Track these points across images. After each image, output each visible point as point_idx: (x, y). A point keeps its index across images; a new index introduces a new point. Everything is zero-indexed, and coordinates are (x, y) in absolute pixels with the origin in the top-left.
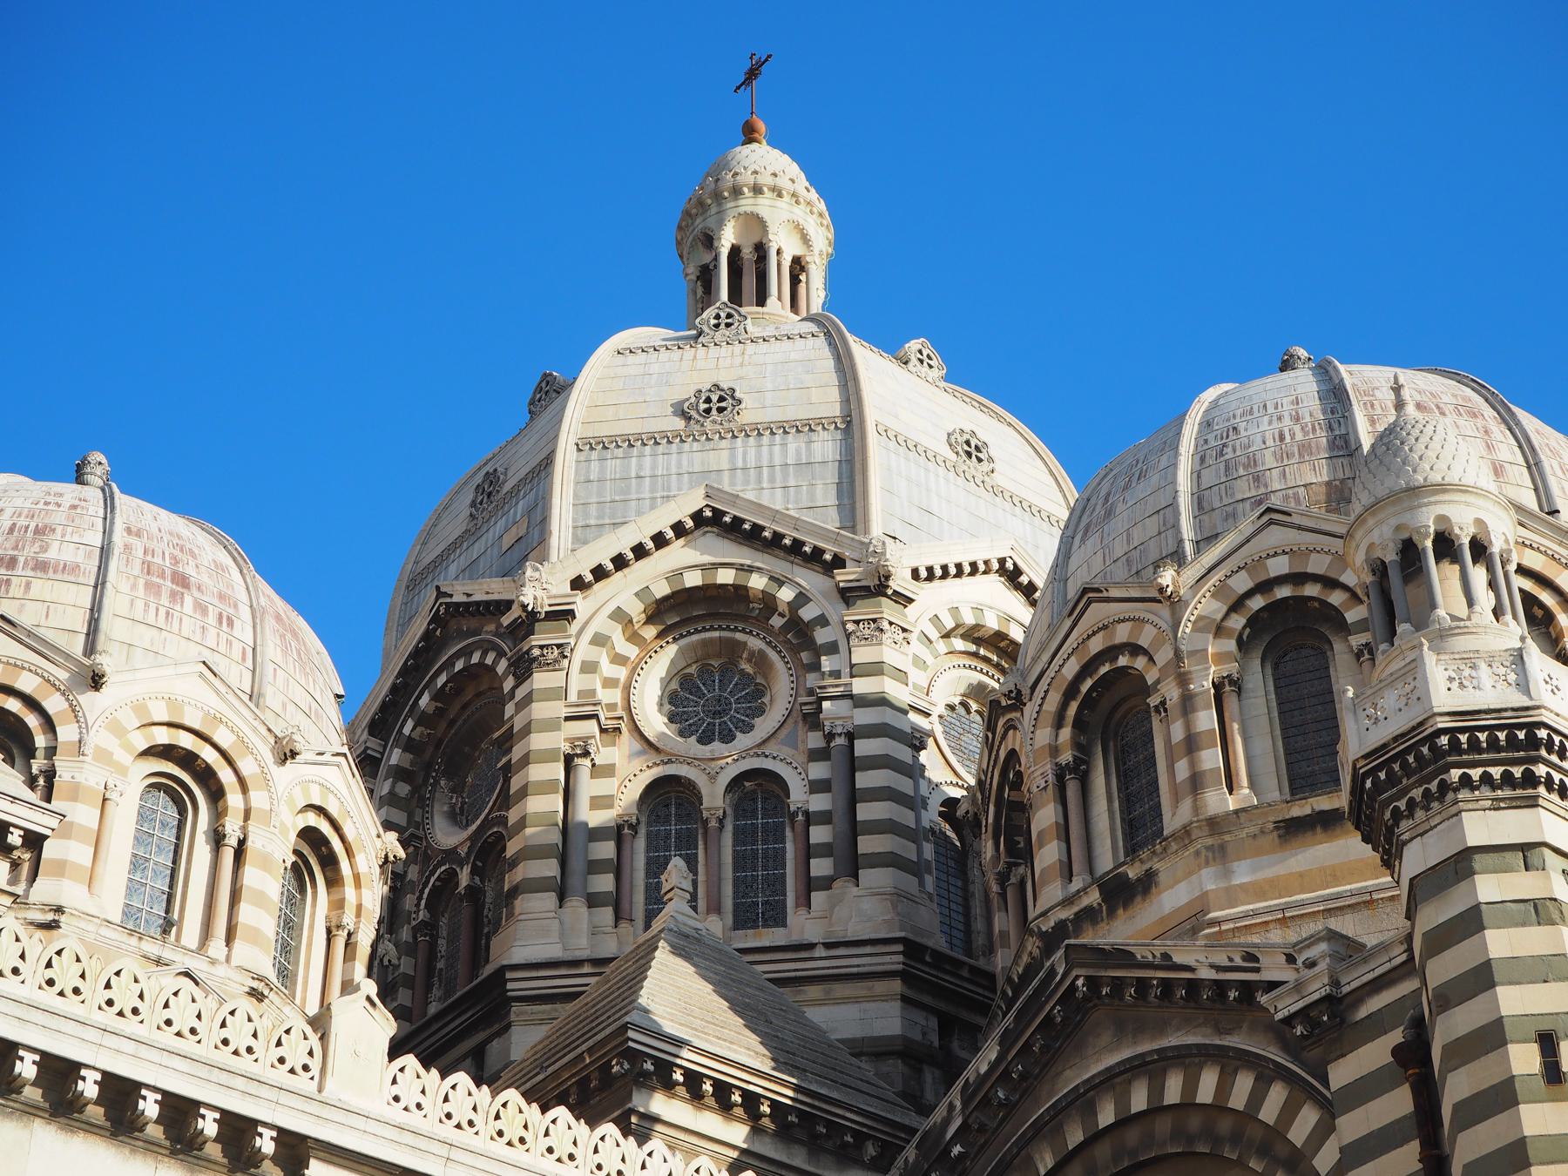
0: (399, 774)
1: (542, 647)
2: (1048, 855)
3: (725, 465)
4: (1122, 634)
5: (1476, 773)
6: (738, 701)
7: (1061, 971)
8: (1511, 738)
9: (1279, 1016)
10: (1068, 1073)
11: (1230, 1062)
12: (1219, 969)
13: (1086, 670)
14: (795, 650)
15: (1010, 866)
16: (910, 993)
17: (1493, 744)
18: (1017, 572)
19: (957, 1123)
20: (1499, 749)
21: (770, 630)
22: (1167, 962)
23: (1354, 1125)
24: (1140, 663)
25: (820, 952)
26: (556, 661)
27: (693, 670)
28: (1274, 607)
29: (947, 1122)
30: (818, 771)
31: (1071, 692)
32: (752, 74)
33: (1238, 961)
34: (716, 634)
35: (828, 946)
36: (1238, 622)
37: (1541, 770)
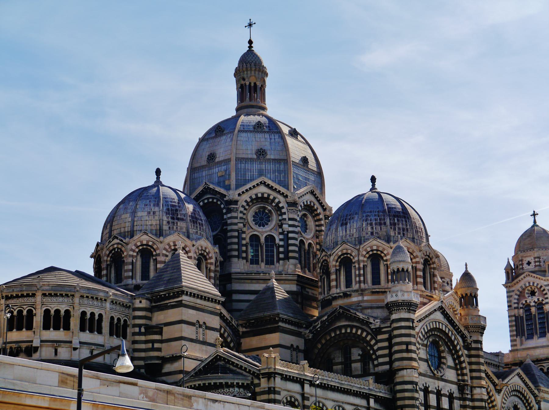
1: (233, 208)
2: (333, 283)
3: (264, 169)
4: (349, 252)
5: (403, 308)
7: (338, 309)
8: (408, 304)
10: (338, 323)
11: (363, 330)
12: (363, 318)
13: (343, 254)
14: (277, 211)
15: (323, 275)
16: (298, 283)
18: (314, 192)
19: (319, 326)
22: (355, 314)
23: (380, 345)
24: (352, 257)
25: (284, 275)
26: (236, 211)
27: (257, 211)
28: (373, 254)
29: (318, 325)
30: (281, 237)
31: (339, 257)
32: (250, 25)
33: (366, 318)
34: (262, 205)
36: (367, 256)
37: (411, 308)
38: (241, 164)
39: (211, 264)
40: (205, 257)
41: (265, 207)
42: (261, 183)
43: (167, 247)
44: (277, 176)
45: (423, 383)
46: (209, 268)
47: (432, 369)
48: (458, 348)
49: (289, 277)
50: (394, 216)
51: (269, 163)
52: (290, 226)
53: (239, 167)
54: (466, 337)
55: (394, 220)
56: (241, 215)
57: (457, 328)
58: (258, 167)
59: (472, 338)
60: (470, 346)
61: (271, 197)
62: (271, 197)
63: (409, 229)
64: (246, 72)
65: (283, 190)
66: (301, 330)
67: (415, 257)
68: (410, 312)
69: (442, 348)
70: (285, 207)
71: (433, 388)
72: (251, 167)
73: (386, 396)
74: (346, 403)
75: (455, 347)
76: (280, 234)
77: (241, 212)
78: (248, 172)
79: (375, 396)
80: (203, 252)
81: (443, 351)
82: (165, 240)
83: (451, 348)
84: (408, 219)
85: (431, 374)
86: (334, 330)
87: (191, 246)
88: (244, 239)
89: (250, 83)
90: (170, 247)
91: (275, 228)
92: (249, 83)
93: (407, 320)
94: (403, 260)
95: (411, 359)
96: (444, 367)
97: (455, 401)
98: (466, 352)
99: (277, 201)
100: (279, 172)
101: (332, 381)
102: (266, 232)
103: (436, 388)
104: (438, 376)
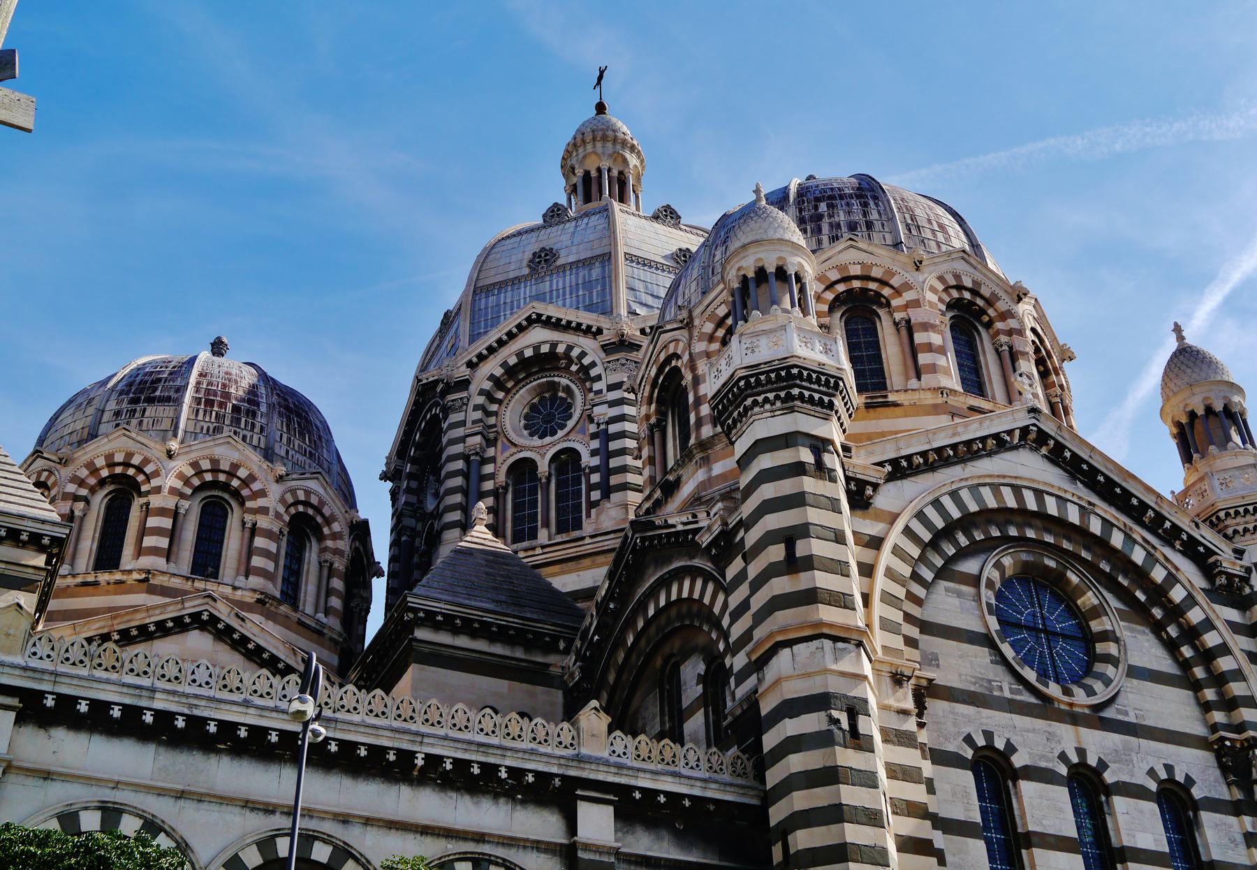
0: (411, 476)
1: (453, 401)
3: (548, 289)
5: (760, 399)
6: (541, 413)
8: (778, 376)
9: (704, 546)
17: (769, 381)
20: (773, 383)
21: (571, 373)
25: (588, 540)
26: (461, 407)
29: (591, 624)
30: (595, 444)
33: (691, 519)
34: (545, 380)
35: (592, 537)
37: (796, 391)
38: (487, 297)
39: (264, 511)
40: (236, 494)
41: (553, 382)
42: (529, 319)
43: (84, 473)
44: (581, 298)
45: (966, 730)
46: (249, 525)
47: (1030, 675)
48: (1177, 594)
49: (606, 543)
50: (818, 200)
51: (561, 274)
52: (612, 404)
53: (483, 307)
54: (1210, 553)
55: (816, 208)
56: (478, 415)
57: (1152, 520)
58: (531, 291)
59: (1246, 556)
60: (1247, 590)
61: (561, 349)
62: (561, 349)
63: (877, 225)
64: (574, 154)
65: (586, 318)
66: (552, 659)
67: (898, 292)
68: (792, 410)
69: (1089, 599)
70: (598, 361)
71: (1042, 757)
72: (512, 297)
73: (709, 794)
74: (368, 821)
75: (1159, 593)
76: (594, 436)
77: (476, 408)
78: (505, 311)
79: (623, 791)
80: (222, 477)
81: (1097, 612)
82: (79, 454)
83: (1141, 597)
84: (875, 198)
85: (1018, 698)
86: (631, 622)
87: (164, 456)
88: (491, 476)
89: (587, 173)
90: (94, 471)
91: (578, 426)
92: (582, 171)
93: (787, 440)
94: (758, 237)
95: (811, 597)
96: (1110, 670)
97: (1205, 816)
98: (1233, 615)
99: (575, 353)
100: (588, 285)
101: (246, 704)
102: (553, 444)
103: (1063, 757)
104: (1071, 705)
